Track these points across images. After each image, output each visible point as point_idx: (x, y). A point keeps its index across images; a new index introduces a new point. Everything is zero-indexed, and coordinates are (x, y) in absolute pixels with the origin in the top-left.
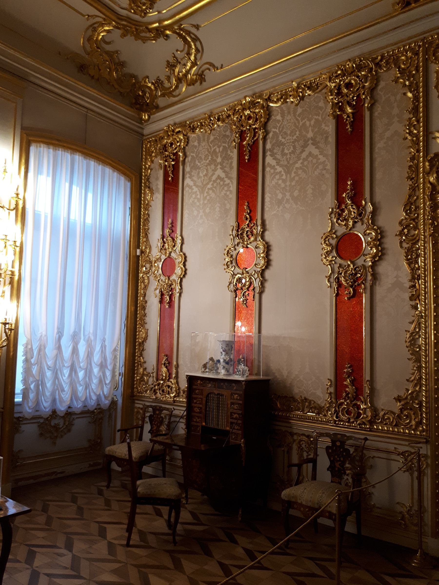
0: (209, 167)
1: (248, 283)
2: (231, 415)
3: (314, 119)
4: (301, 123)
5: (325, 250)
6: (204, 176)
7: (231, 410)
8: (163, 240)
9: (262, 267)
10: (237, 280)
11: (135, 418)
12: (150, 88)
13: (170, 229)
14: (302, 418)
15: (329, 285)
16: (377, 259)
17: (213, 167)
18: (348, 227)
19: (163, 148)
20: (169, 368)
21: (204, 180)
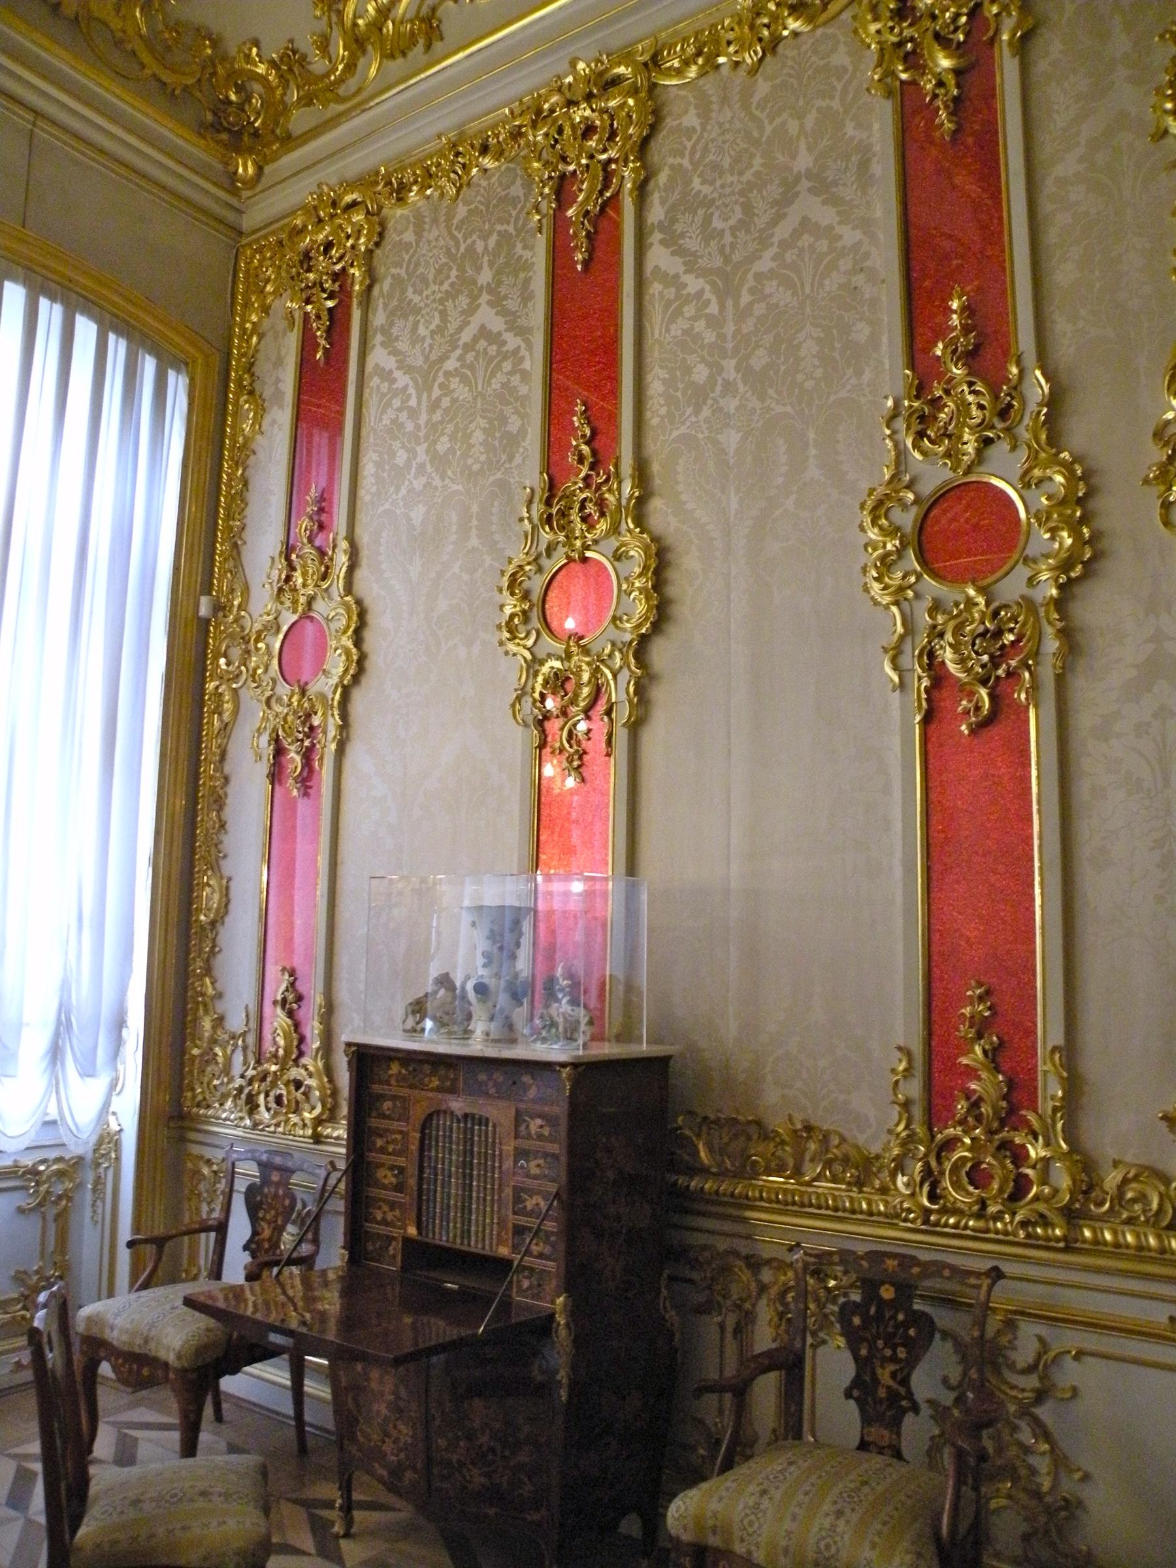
0: (449, 304)
1: (586, 691)
3: (814, 111)
4: (769, 129)
5: (875, 549)
6: (432, 332)
8: (288, 558)
12: (263, 79)
13: (311, 518)
14: (794, 1203)
15: (896, 679)
16: (1080, 569)
17: (463, 301)
18: (959, 461)
19: (301, 262)
21: (431, 346)
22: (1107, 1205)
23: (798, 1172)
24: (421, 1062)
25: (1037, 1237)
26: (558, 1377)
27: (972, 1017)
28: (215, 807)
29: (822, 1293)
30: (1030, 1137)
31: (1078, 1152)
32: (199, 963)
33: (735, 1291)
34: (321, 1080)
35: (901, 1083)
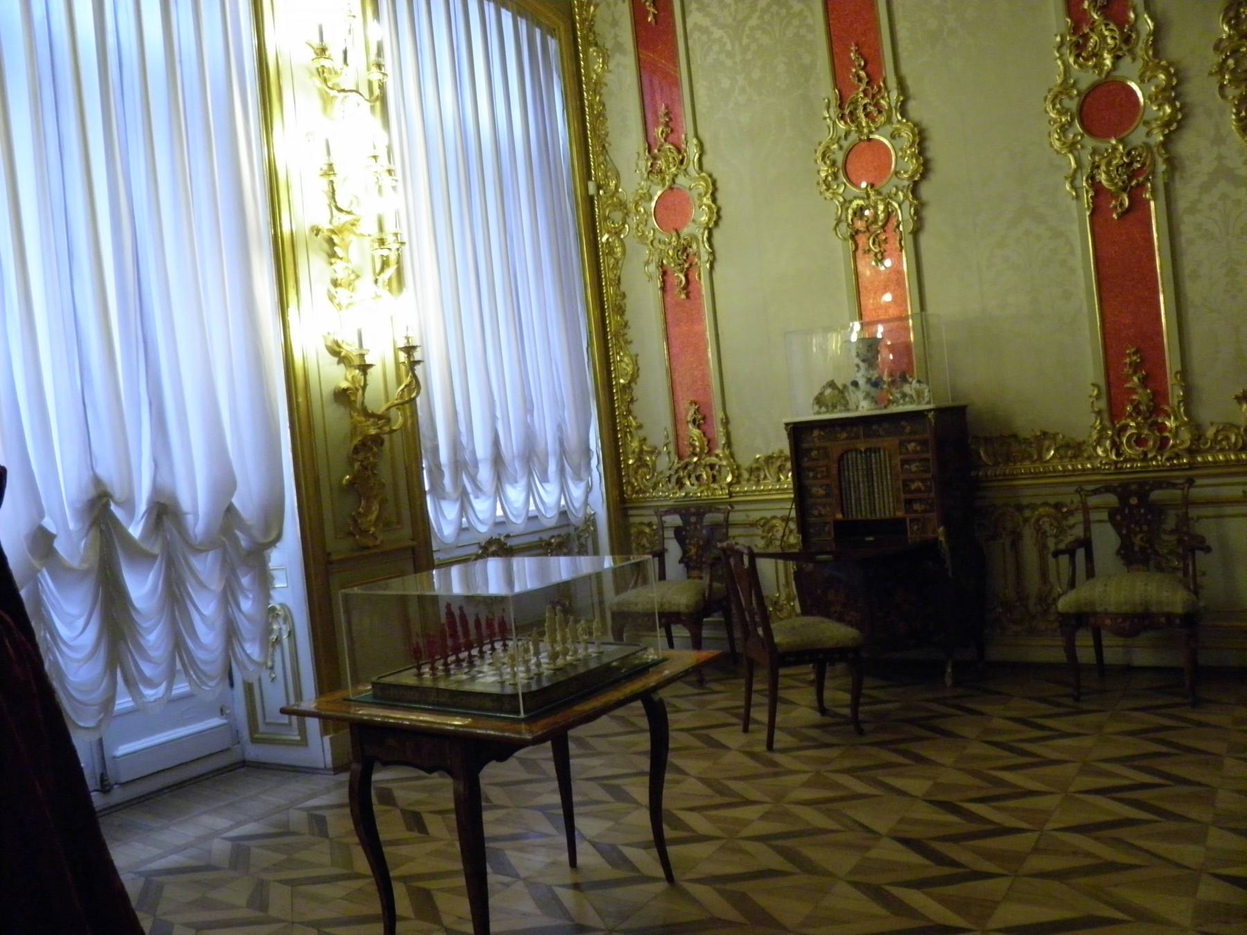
9: (912, 177)
10: (855, 213)
11: (634, 545)
16: (1175, 127)
21: (736, 11)
23: (1040, 457)
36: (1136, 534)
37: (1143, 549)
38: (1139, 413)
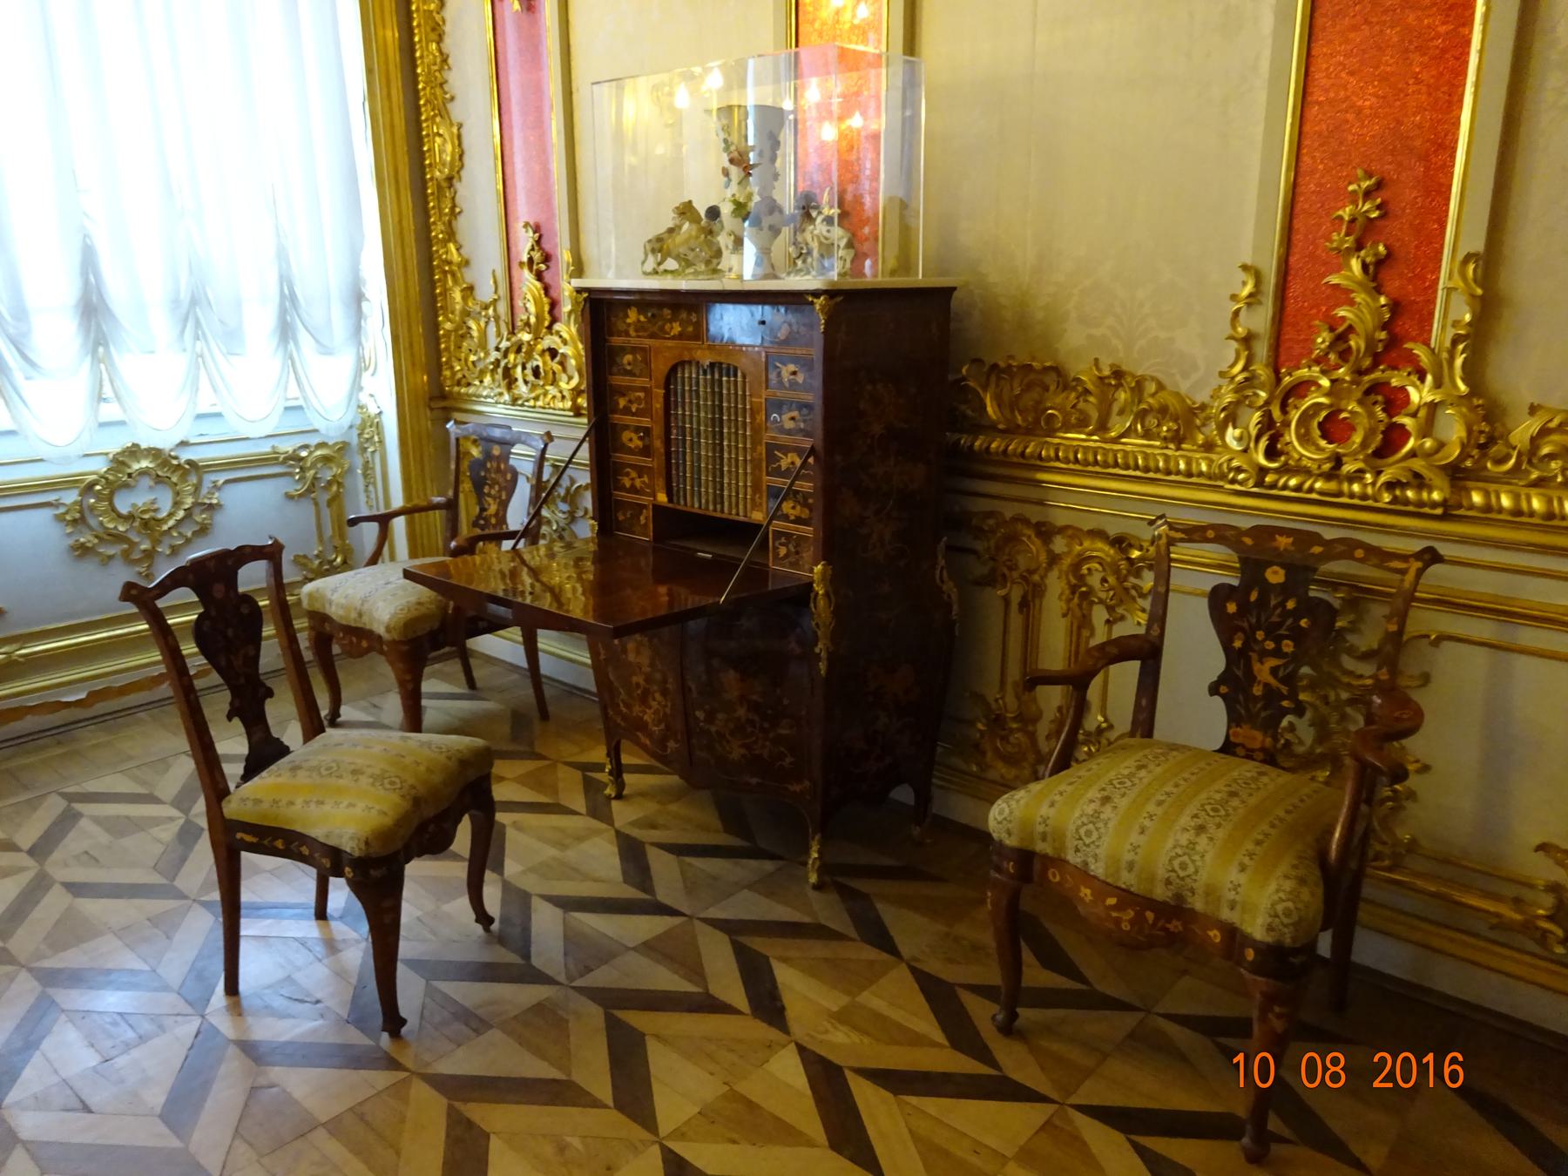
2: (771, 459)
7: (767, 437)
14: (1096, 463)
20: (547, 277)
22: (1512, 461)
23: (1102, 427)
24: (660, 305)
25: (1407, 502)
26: (817, 650)
27: (1353, 221)
28: (434, 36)
29: (1123, 565)
30: (1414, 378)
31: (1480, 396)
32: (440, 227)
33: (1023, 562)
34: (576, 347)
35: (1243, 314)
36: (1264, 654)
37: (1271, 695)
38: (1344, 355)
